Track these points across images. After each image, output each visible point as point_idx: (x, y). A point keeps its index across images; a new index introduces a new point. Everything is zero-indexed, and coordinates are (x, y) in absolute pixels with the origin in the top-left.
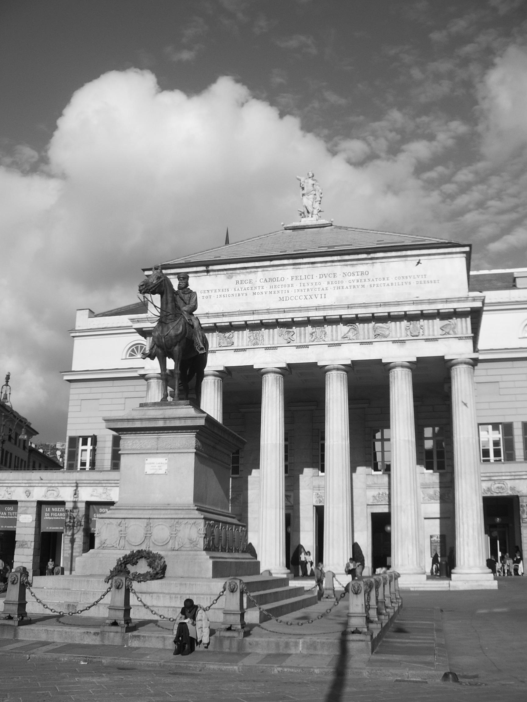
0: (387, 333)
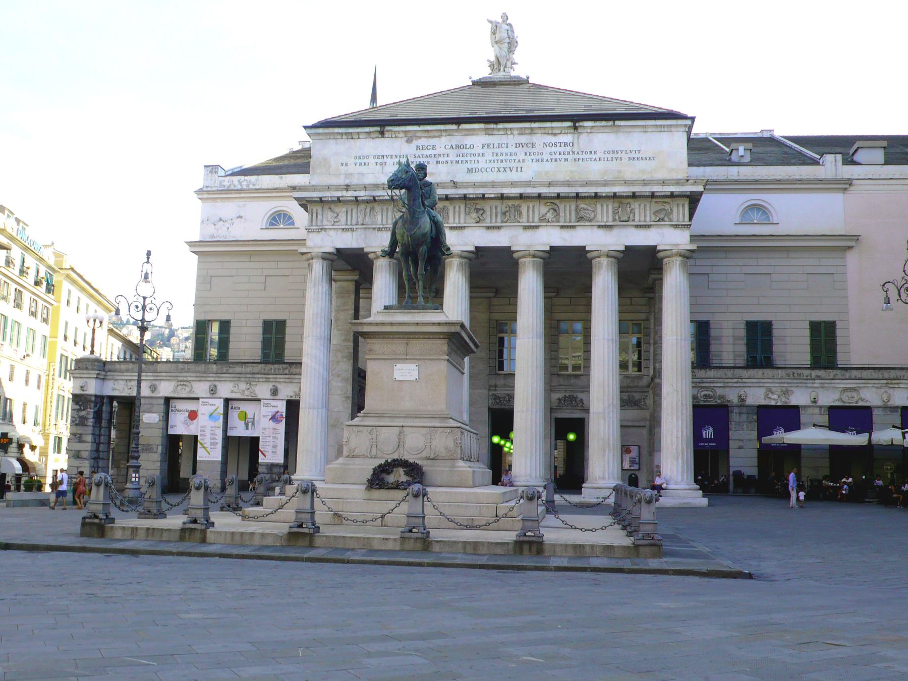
0: (592, 216)
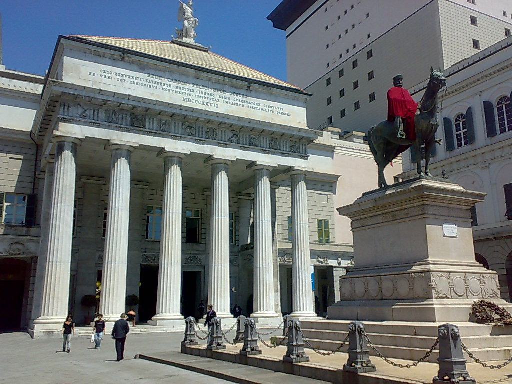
0: (258, 143)
